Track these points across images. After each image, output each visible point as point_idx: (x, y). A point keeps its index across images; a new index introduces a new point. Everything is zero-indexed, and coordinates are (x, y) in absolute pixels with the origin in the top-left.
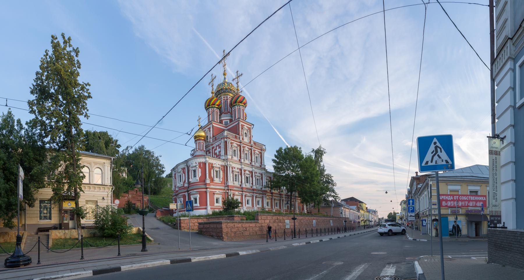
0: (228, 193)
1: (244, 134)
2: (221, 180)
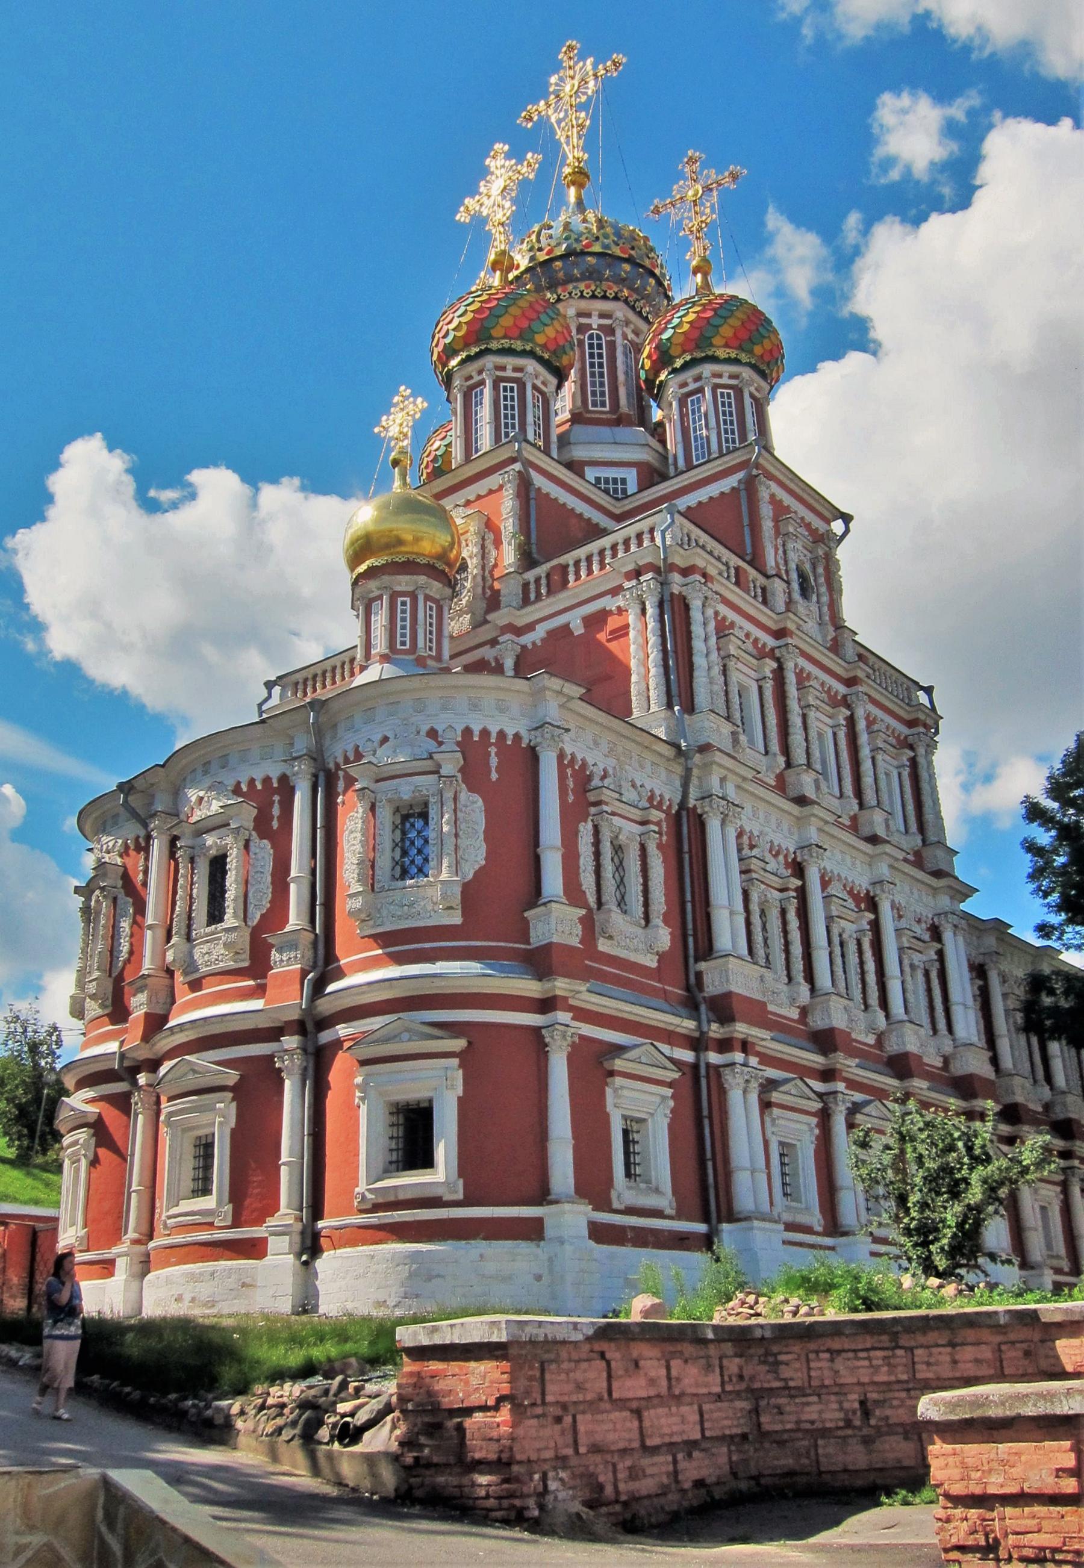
0: (716, 1071)
1: (794, 576)
2: (664, 937)
